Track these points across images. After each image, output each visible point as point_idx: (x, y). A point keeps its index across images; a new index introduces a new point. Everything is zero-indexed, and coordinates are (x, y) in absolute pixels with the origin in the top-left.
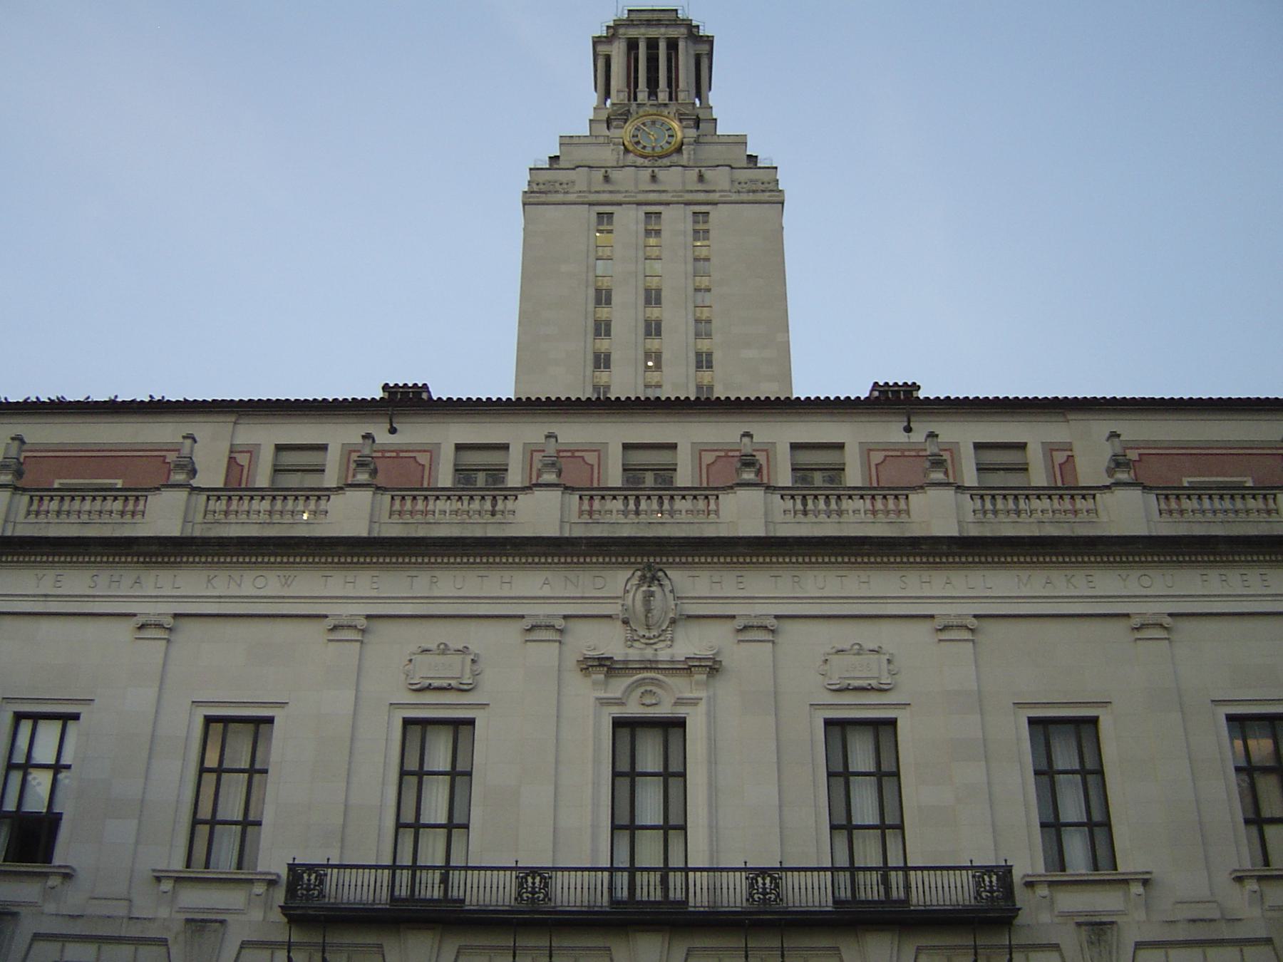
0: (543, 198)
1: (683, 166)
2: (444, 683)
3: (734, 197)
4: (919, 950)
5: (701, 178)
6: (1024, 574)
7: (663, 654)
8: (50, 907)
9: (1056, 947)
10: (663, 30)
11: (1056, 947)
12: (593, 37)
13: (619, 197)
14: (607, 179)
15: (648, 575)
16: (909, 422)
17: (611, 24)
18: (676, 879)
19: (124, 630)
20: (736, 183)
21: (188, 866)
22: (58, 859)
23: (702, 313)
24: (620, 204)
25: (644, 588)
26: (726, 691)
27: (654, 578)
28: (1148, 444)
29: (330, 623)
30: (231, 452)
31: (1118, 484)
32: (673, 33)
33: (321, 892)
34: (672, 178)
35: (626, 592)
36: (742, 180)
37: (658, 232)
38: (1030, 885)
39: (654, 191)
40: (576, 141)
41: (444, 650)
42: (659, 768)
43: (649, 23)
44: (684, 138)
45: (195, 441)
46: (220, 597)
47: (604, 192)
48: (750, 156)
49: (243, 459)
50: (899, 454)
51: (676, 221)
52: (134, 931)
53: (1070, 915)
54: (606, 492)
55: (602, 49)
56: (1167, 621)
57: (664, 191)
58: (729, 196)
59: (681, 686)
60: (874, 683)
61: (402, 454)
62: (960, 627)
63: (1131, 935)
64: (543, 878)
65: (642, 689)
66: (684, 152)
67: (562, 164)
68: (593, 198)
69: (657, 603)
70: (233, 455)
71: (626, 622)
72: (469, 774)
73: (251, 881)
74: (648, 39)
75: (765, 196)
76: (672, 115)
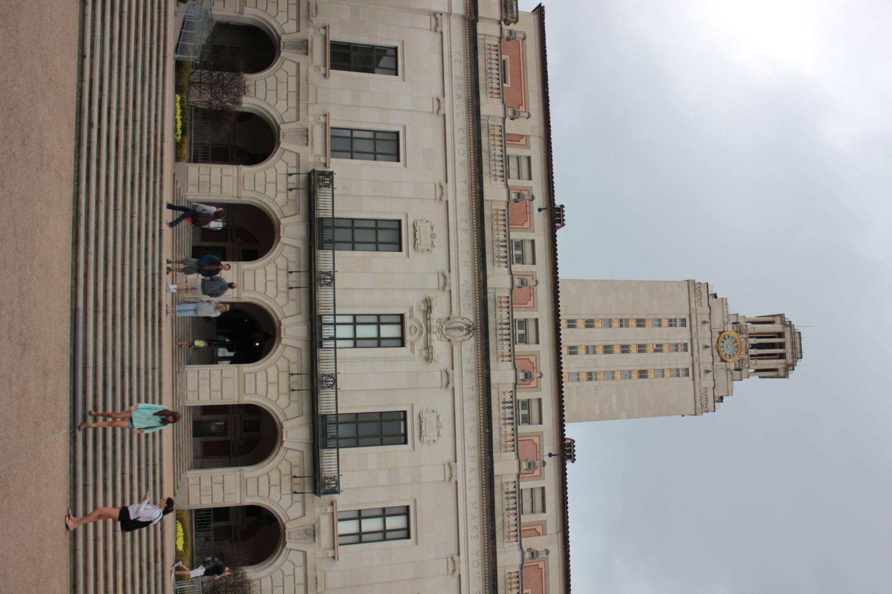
0: (692, 290)
1: (713, 363)
2: (418, 237)
3: (697, 390)
4: (303, 452)
5: (707, 372)
6: (478, 505)
7: (434, 336)
8: (311, 69)
9: (304, 515)
10: (790, 351)
11: (304, 515)
12: (784, 314)
14: (704, 322)
15: (471, 329)
16: (554, 455)
17: (792, 323)
18: (331, 344)
19: (437, 92)
20: (705, 390)
21: (332, 128)
22: (331, 71)
23: (635, 374)
24: (691, 330)
25: (464, 327)
26: (418, 364)
27: (469, 331)
28: (547, 573)
29: (444, 184)
30: (526, 136)
31: (523, 553)
32: (789, 356)
33: (321, 186)
34: (706, 357)
35: (463, 319)
36: (707, 394)
37: (677, 350)
38: (332, 504)
39: (699, 347)
40: (725, 306)
41: (433, 236)
42: (383, 335)
43: (793, 343)
44: (729, 363)
45: (528, 118)
46: (454, 134)
47: (697, 322)
48: (722, 398)
49: (523, 141)
50: (538, 450)
51: (683, 360)
52: (302, 106)
53: (318, 521)
54: (510, 310)
55: (778, 319)
56: (456, 573)
57: (699, 353)
58: (698, 386)
59: (420, 344)
60: (423, 434)
61: (528, 215)
62: (451, 474)
63: (310, 549)
64: (330, 283)
65: (417, 327)
66: (721, 363)
67: (712, 300)
68: (693, 315)
69: (458, 333)
70: (525, 137)
71: (449, 319)
72: (377, 250)
73: (326, 156)
74: (785, 343)
75: (698, 405)
76: (742, 356)
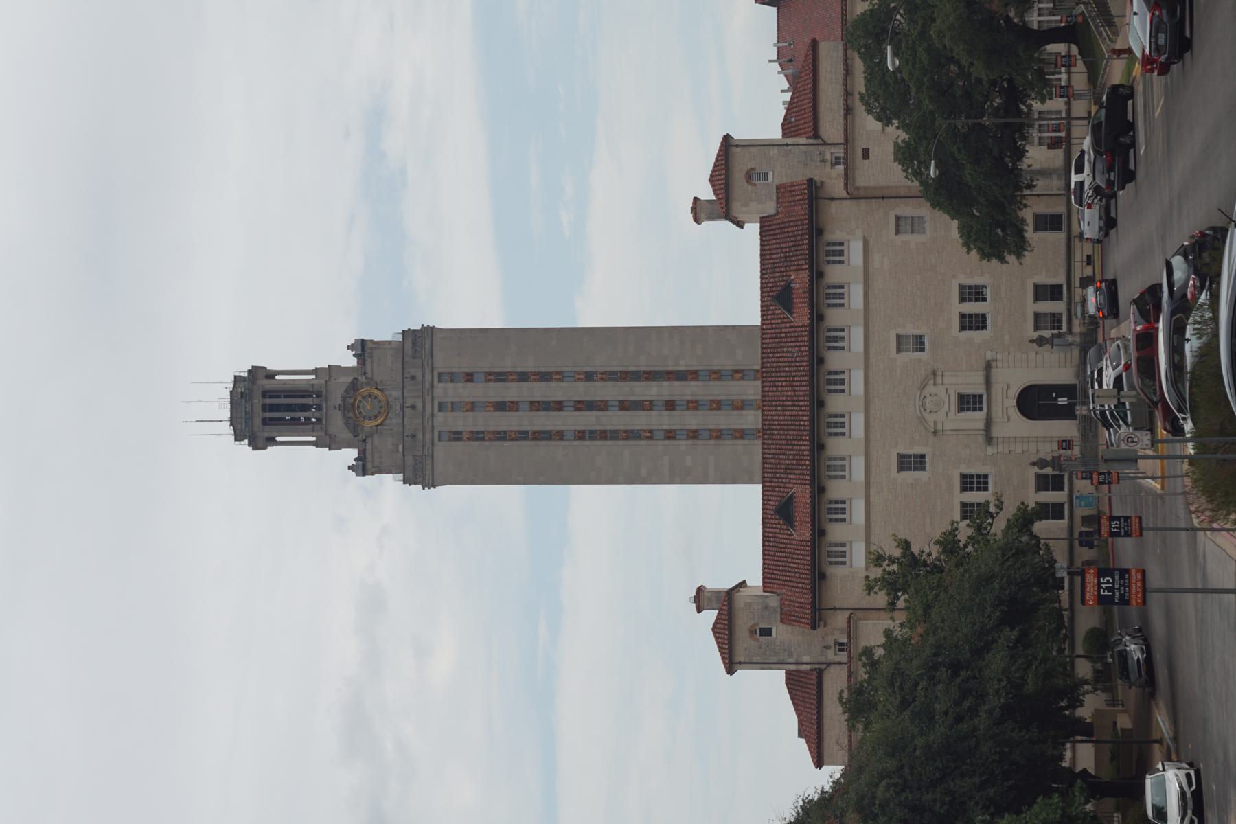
13: (428, 429)
